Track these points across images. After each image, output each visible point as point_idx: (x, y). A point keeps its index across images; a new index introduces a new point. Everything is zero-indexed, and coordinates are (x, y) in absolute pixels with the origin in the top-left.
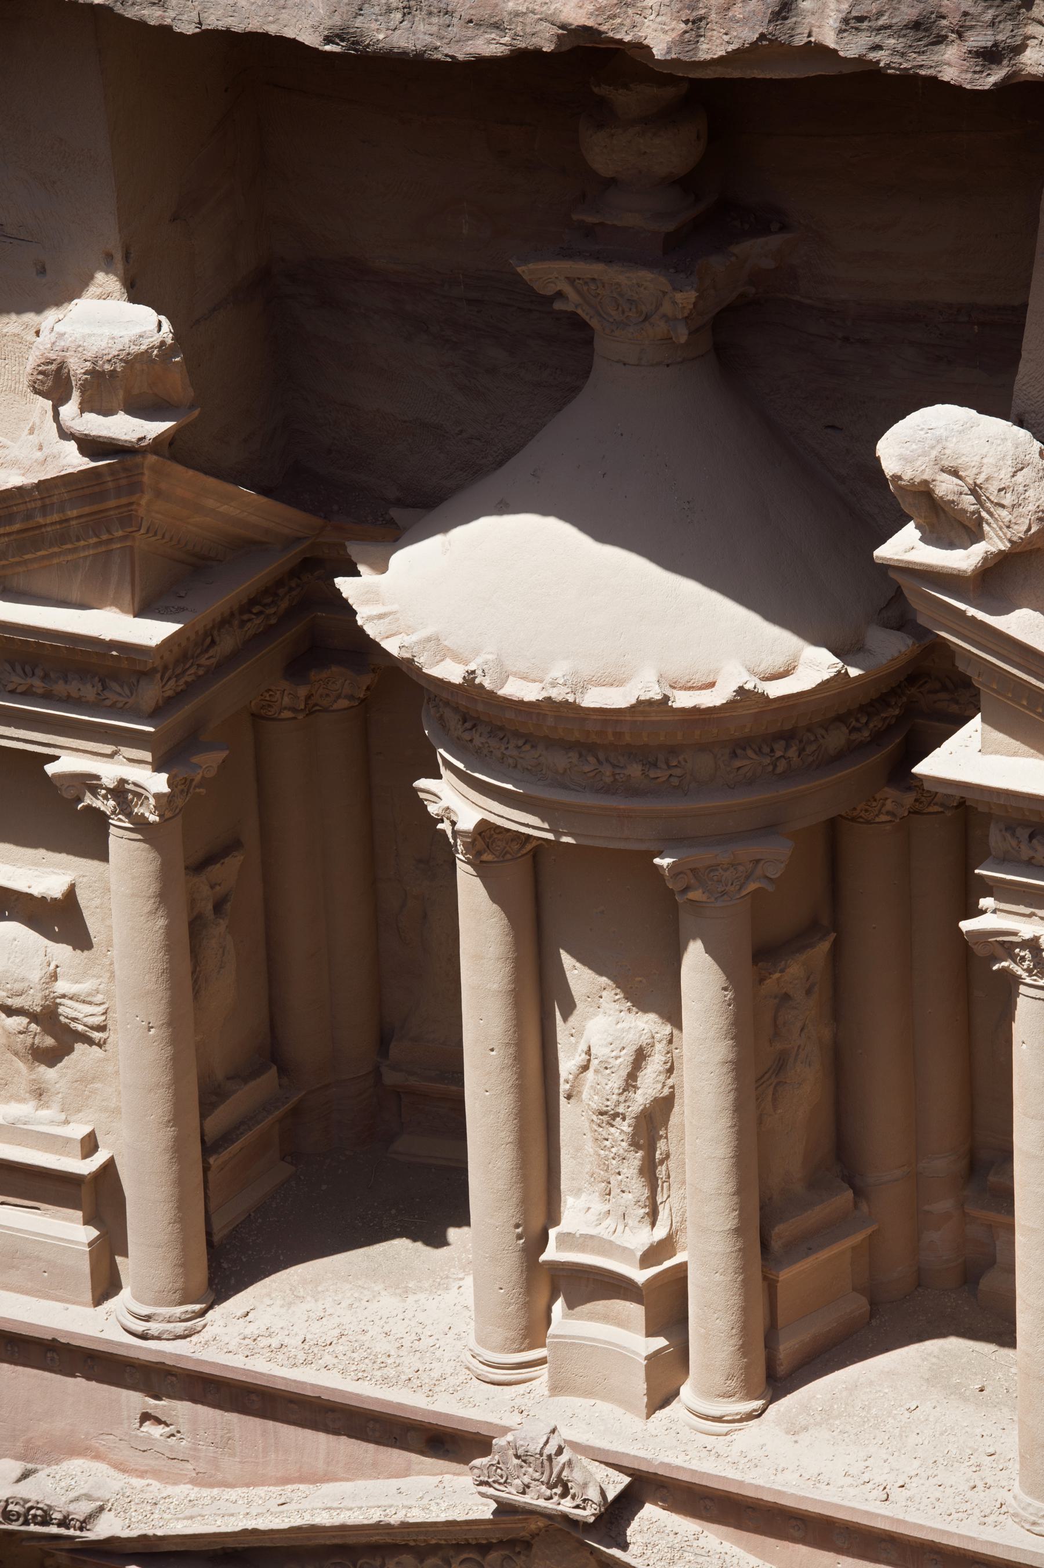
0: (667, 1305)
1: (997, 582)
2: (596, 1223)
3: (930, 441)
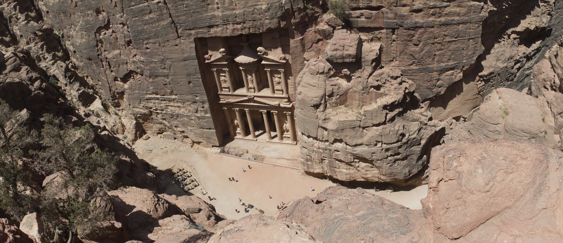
0: (254, 88)
1: (263, 54)
2: (251, 85)
3: (259, 49)
